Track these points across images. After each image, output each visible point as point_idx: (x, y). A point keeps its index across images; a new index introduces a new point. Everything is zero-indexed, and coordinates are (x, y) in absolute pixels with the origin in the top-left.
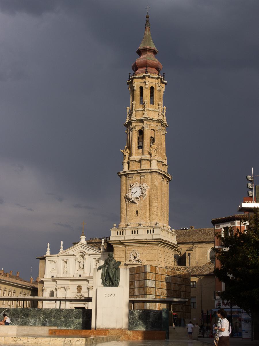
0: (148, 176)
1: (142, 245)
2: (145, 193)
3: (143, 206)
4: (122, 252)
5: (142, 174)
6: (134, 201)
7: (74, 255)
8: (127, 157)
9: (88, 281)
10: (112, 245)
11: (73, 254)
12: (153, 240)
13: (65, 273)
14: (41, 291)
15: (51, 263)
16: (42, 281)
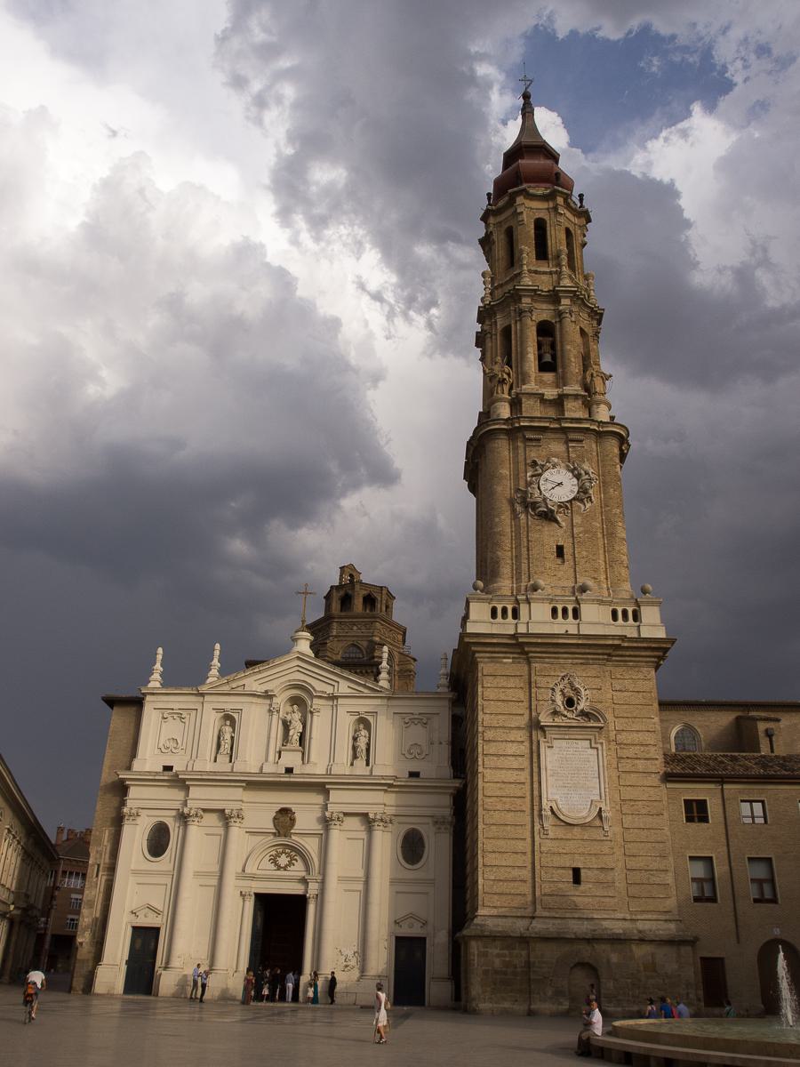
0: (590, 444)
1: (599, 659)
2: (591, 492)
3: (586, 532)
4: (512, 680)
5: (572, 436)
6: (552, 511)
7: (268, 696)
8: (506, 388)
9: (326, 793)
10: (475, 652)
11: (266, 692)
12: (645, 645)
13: (223, 759)
14: (108, 824)
15: (164, 718)
16: (123, 781)
